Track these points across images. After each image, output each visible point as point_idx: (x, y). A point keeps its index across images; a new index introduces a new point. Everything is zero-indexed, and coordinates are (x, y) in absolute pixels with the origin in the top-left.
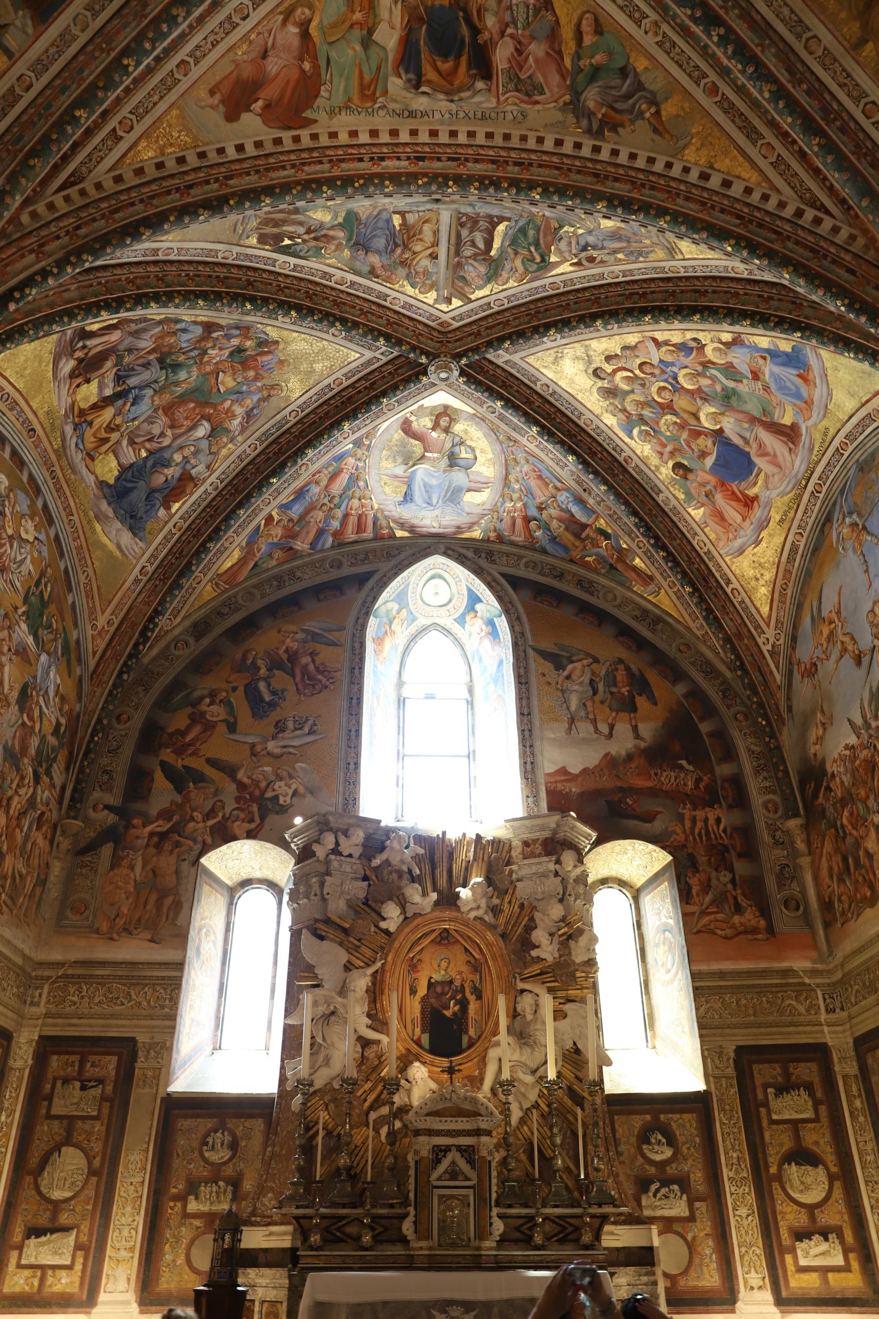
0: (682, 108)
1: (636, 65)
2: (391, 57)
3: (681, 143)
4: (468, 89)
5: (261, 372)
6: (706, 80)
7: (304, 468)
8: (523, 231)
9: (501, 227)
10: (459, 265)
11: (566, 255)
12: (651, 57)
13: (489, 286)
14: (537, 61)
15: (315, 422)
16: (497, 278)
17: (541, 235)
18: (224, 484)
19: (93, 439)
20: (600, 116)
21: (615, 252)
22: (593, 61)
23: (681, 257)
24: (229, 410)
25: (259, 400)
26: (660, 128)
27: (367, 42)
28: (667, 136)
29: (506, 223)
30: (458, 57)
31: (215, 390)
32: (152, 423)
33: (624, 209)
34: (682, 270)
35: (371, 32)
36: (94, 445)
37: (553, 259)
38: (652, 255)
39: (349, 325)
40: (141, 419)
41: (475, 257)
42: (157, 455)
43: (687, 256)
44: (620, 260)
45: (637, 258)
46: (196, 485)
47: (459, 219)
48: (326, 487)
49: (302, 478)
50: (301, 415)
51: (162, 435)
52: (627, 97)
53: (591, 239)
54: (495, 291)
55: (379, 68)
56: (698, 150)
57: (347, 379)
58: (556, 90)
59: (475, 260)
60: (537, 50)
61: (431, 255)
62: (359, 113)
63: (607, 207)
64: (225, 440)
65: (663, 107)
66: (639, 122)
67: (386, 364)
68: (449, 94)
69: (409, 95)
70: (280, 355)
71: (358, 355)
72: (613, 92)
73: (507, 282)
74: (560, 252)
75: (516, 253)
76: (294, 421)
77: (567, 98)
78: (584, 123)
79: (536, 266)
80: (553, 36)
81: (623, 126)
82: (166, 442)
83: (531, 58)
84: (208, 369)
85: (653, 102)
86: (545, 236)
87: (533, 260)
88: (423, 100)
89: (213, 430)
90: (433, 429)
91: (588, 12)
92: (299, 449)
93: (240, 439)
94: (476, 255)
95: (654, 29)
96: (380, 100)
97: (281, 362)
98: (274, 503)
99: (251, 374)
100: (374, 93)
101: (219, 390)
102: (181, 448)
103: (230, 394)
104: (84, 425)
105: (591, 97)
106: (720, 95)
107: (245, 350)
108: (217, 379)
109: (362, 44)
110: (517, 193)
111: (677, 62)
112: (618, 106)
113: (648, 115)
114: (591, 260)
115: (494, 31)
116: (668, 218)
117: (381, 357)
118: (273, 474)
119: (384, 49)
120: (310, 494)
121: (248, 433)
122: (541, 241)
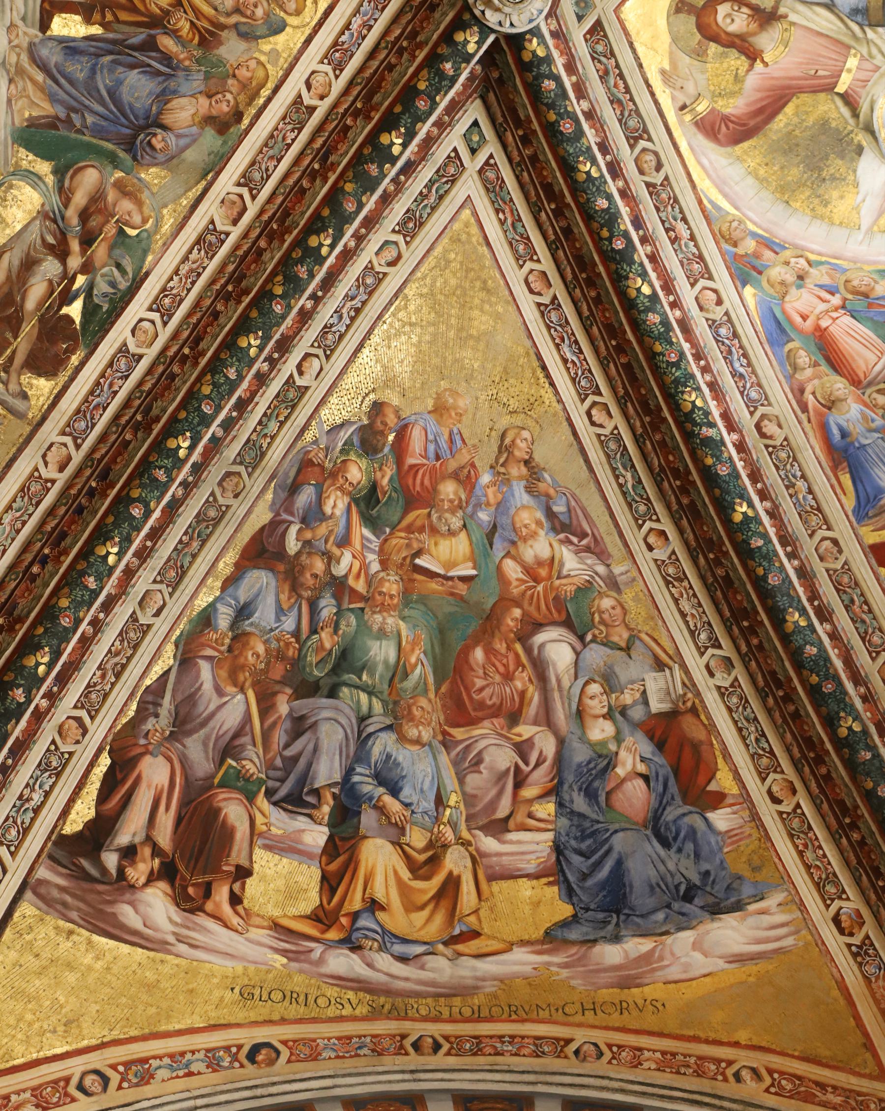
5: (453, 465)
7: (770, 428)
15: (628, 367)
18: (724, 641)
19: (426, 913)
24: (530, 572)
25: (529, 490)
31: (462, 589)
32: (478, 761)
36: (439, 919)
39: (326, 212)
40: (450, 782)
42: (570, 778)
46: (694, 711)
48: (855, 382)
49: (799, 439)
50: (607, 397)
51: (522, 749)
57: (532, 255)
64: (606, 603)
67: (505, 146)
70: (417, 408)
71: (466, 213)
76: (618, 419)
82: (547, 745)
84: (392, 585)
89: (568, 624)
90: (753, 55)
92: (680, 425)
93: (617, 570)
97: (440, 410)
98: (843, 529)
99: (449, 489)
101: (464, 579)
102: (580, 714)
103: (487, 556)
104: (362, 922)
107: (374, 487)
108: (431, 575)
117: (482, 157)
118: (724, 509)
120: (857, 429)
121: (612, 543)
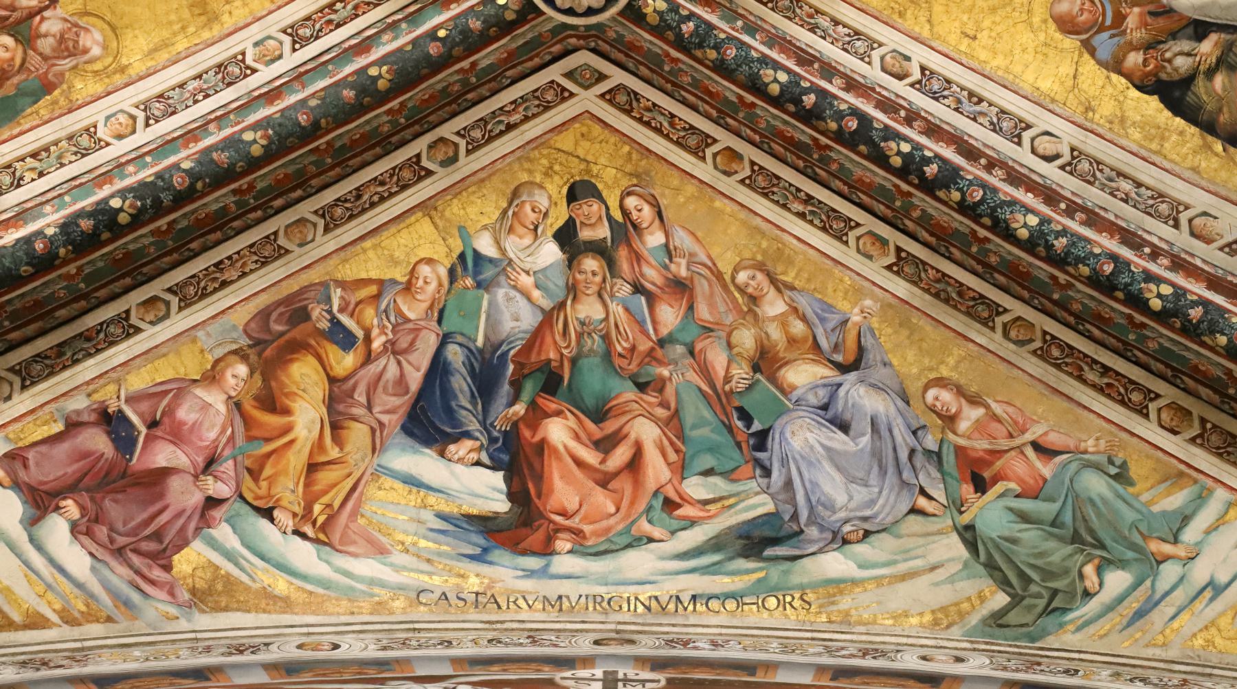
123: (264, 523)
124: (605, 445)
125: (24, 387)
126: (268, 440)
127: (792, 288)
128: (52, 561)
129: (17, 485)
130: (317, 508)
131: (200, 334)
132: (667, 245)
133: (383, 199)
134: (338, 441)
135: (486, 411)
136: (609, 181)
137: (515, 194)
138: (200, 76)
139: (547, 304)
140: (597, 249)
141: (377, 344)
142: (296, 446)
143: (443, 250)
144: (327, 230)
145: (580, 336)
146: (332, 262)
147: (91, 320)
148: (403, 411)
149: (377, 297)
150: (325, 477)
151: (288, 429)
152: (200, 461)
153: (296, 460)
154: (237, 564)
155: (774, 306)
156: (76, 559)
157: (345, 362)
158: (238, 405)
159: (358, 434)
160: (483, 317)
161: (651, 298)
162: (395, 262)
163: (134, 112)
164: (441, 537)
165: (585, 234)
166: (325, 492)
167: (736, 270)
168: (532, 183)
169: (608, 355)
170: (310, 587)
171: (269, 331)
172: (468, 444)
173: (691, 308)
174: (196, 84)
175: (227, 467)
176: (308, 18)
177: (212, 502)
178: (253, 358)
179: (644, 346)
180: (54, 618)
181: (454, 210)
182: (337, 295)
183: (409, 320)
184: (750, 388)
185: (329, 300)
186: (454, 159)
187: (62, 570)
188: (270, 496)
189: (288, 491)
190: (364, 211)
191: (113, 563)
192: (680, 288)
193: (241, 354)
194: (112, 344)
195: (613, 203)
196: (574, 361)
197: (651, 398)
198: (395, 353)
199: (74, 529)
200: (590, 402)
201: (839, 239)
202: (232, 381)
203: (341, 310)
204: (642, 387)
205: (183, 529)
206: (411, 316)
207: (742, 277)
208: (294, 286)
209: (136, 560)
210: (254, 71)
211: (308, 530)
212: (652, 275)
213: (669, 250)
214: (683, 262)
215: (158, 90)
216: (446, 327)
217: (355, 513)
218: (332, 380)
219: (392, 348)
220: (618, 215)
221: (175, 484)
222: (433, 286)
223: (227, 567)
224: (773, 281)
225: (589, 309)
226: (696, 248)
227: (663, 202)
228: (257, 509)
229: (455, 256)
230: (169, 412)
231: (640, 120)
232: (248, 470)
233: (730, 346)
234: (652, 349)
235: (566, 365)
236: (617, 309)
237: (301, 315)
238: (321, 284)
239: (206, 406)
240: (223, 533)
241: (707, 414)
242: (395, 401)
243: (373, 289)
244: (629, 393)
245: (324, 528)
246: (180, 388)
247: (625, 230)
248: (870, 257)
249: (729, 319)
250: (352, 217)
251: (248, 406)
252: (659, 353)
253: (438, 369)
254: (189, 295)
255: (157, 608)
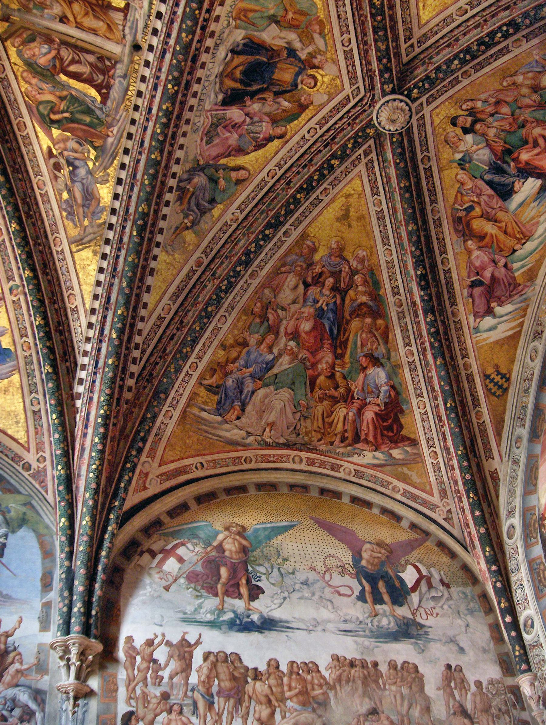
0: (189, 245)
1: (216, 209)
2: (256, 34)
3: (169, 248)
4: (220, 89)
6: (204, 258)
8: (89, 111)
9: (93, 92)
10: (49, 40)
11: (61, 145)
12: (219, 219)
13: (19, 62)
14: (227, 139)
16: (31, 73)
17: (84, 127)
20: (188, 187)
21: (69, 191)
22: (221, 179)
23: (74, 249)
26: (178, 232)
27: (274, 19)
28: (173, 237)
29: (99, 99)
30: (241, 81)
33: (142, 226)
34: (59, 249)
35: (277, 22)
37: (56, 132)
38: (71, 224)
41: (58, 57)
43: (76, 256)
44: (60, 195)
45: (65, 210)
47: (109, 59)
52: (198, 205)
53: (82, 172)
54: (16, 68)
55: (253, 24)
56: (165, 261)
58: (207, 154)
59: (54, 58)
60: (233, 139)
61: (66, 17)
62: (231, 6)
63: (143, 212)
65: (190, 231)
66: (181, 215)
68: (221, 76)
69: (229, 44)
72: (201, 195)
73: (26, 82)
74: (65, 140)
75: (62, 98)
77: (202, 162)
78: (185, 176)
79: (46, 113)
80: (240, 151)
81: (181, 204)
83: (229, 134)
85: (194, 223)
86: (82, 130)
87: (53, 110)
88: (223, 55)
91: (249, 174)
94: (62, 60)
95: (235, 218)
96: (234, 23)
100: (240, 19)
105: (200, 180)
106: (197, 269)
109: (274, 15)
110: (158, 140)
111: (215, 236)
112: (193, 199)
113: (186, 221)
114: (57, 167)
115: (250, 109)
116: (136, 261)
119: (264, 30)
122: (76, 126)
123: (517, 253)
124: (536, 144)
125: (457, 305)
126: (493, 242)
127: (517, 72)
128: (507, 314)
129: (483, 317)
130: (518, 236)
131: (456, 251)
132: (483, 102)
133: (433, 183)
134: (500, 222)
135: (508, 174)
136: (453, 112)
137: (446, 141)
138: (379, 226)
139: (484, 144)
140: (474, 123)
141: (476, 199)
142: (498, 236)
143: (455, 169)
144: (437, 203)
145: (498, 138)
146: (447, 205)
147: (443, 281)
148: (498, 198)
149: (462, 194)
150: (509, 230)
151: (492, 235)
152: (493, 264)
153: (502, 237)
154: (526, 266)
155: (520, 79)
156: (509, 308)
157: (478, 211)
158: (480, 247)
159: (500, 215)
160: (480, 164)
161: (496, 113)
162: (453, 186)
163: (385, 248)
164: (541, 204)
165: (468, 125)
166: (514, 232)
167: (502, 85)
168: (445, 136)
169: (508, 132)
170: (540, 248)
171: (460, 231)
172: (516, 183)
173: (506, 102)
174: (381, 228)
175: (497, 257)
176: (371, 188)
177: (506, 266)
178: (467, 238)
179: (511, 120)
180: (522, 320)
181: (444, 162)
182: (457, 206)
183: (472, 188)
184: (541, 96)
185: (458, 209)
186: (429, 158)
187: (510, 313)
188: (509, 248)
189: (509, 242)
190: (435, 190)
191: (513, 299)
192: (498, 103)
193: (465, 241)
194: (451, 277)
195: (462, 113)
196: (505, 143)
197: (528, 125)
198: (480, 195)
199: (500, 306)
200: (520, 143)
201: (509, 52)
202: (472, 247)
203: (462, 207)
204: (523, 126)
205: (511, 277)
206: (471, 186)
207: (505, 84)
208: (450, 219)
209: (514, 292)
210: (382, 209)
211: (523, 241)
212: (490, 109)
213: (485, 102)
214: (491, 99)
215: (380, 239)
216: (478, 175)
217: (523, 225)
218: (482, 217)
219: (479, 195)
220: (467, 113)
221: (496, 274)
222: (465, 177)
223: (525, 269)
224: (511, 76)
225: (492, 132)
226: (488, 93)
227: (469, 98)
228: (512, 253)
229: (457, 166)
230: (476, 268)
231: (440, 96)
232: (500, 251)
233: (524, 96)
234: (514, 119)
235: (506, 145)
236: (495, 124)
237: (459, 220)
238: (452, 210)
239: (477, 257)
240: (515, 266)
241: (542, 112)
242: (494, 201)
243: (459, 195)
244: (523, 131)
245: (525, 237)
246: (470, 262)
247: (472, 112)
248: (520, 46)
249: (516, 93)
250: (436, 195)
251: (481, 244)
252: (515, 117)
253: (490, 184)
254: (443, 250)
255: (529, 292)
